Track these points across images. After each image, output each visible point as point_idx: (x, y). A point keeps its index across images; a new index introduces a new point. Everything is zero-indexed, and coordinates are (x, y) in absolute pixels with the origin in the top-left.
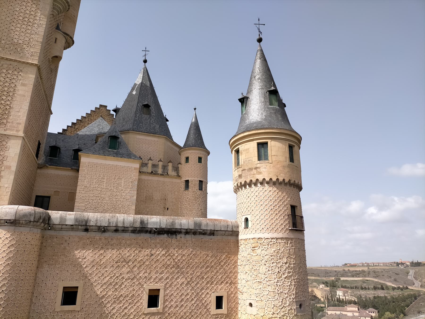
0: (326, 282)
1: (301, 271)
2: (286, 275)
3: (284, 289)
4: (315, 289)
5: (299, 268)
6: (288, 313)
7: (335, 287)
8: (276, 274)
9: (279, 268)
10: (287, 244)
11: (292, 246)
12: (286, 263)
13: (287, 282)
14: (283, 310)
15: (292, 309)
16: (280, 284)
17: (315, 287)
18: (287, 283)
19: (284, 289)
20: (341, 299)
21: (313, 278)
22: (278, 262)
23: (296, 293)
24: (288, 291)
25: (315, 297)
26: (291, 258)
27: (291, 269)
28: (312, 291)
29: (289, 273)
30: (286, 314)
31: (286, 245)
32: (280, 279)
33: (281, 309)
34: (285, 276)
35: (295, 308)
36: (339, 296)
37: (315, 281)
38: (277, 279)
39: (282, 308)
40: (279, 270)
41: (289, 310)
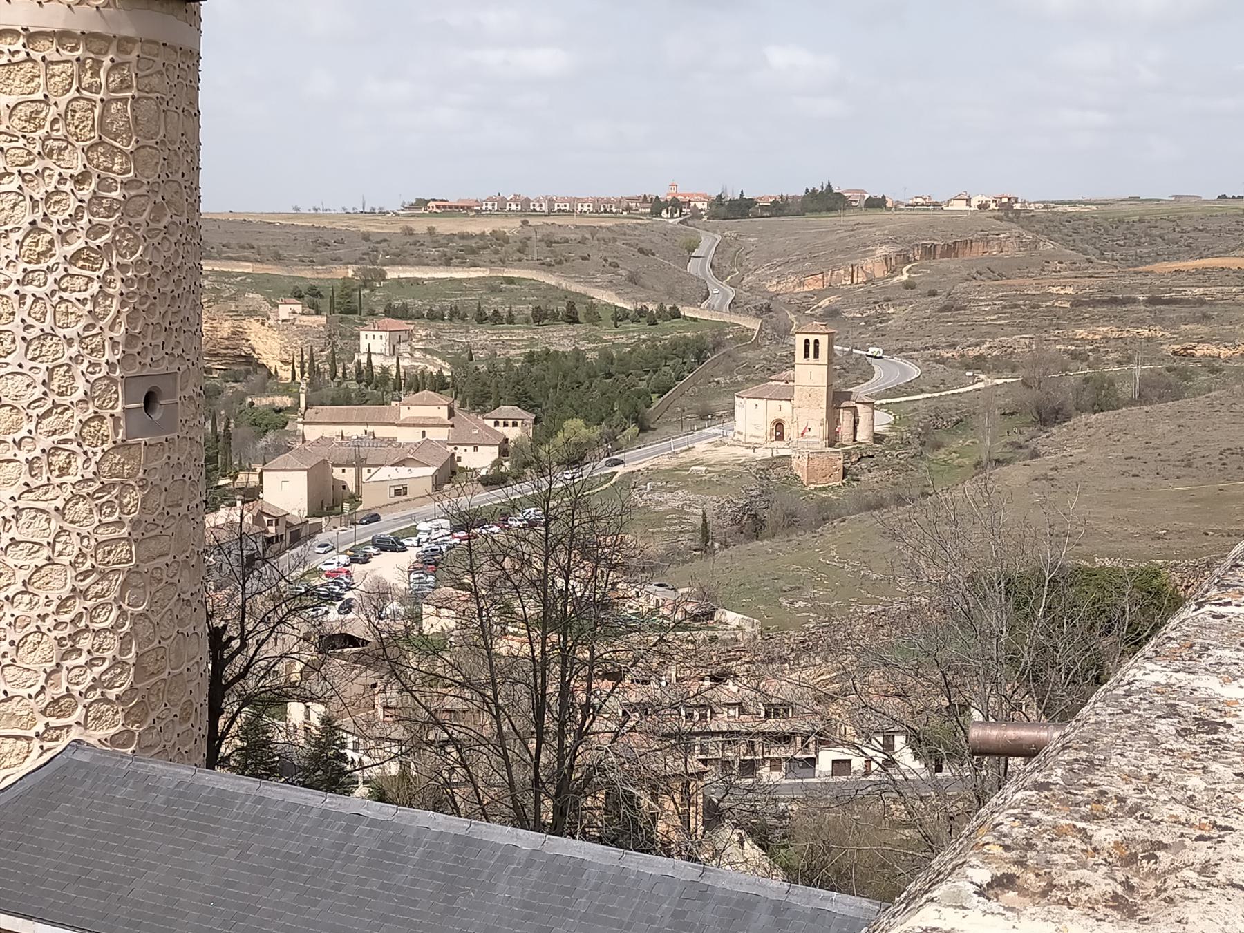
0: (313, 288)
1: (165, 222)
2: (80, 244)
3: (62, 319)
4: (252, 327)
5: (158, 210)
6: (81, 438)
7: (354, 312)
8: (19, 236)
9: (35, 204)
10: (96, 74)
11: (124, 85)
12: (80, 180)
13: (80, 283)
14: (51, 422)
15: (102, 418)
16: (40, 292)
17: (252, 313)
18: (83, 286)
19: (62, 319)
20: (377, 371)
21: (248, 268)
22: (31, 169)
23: (130, 338)
24: (86, 328)
25: (251, 361)
26: (114, 151)
27: (110, 211)
28: (237, 334)
29: (95, 231)
30: (65, 441)
31: (87, 79)
32: (43, 266)
33: (41, 418)
34: (70, 250)
35: (118, 411)
36: (369, 354)
37: (258, 283)
38: (22, 265)
39: (48, 413)
40: (38, 216)
41: (84, 424)
